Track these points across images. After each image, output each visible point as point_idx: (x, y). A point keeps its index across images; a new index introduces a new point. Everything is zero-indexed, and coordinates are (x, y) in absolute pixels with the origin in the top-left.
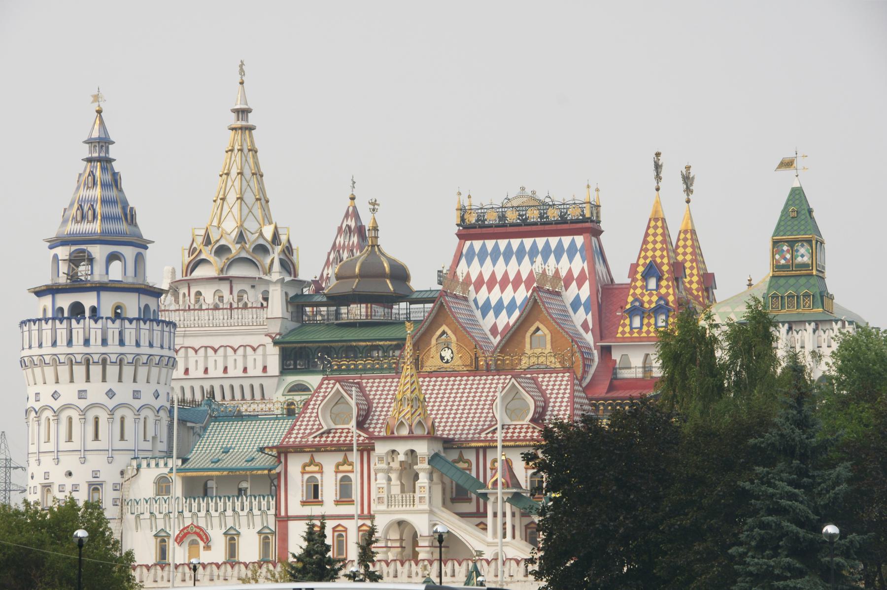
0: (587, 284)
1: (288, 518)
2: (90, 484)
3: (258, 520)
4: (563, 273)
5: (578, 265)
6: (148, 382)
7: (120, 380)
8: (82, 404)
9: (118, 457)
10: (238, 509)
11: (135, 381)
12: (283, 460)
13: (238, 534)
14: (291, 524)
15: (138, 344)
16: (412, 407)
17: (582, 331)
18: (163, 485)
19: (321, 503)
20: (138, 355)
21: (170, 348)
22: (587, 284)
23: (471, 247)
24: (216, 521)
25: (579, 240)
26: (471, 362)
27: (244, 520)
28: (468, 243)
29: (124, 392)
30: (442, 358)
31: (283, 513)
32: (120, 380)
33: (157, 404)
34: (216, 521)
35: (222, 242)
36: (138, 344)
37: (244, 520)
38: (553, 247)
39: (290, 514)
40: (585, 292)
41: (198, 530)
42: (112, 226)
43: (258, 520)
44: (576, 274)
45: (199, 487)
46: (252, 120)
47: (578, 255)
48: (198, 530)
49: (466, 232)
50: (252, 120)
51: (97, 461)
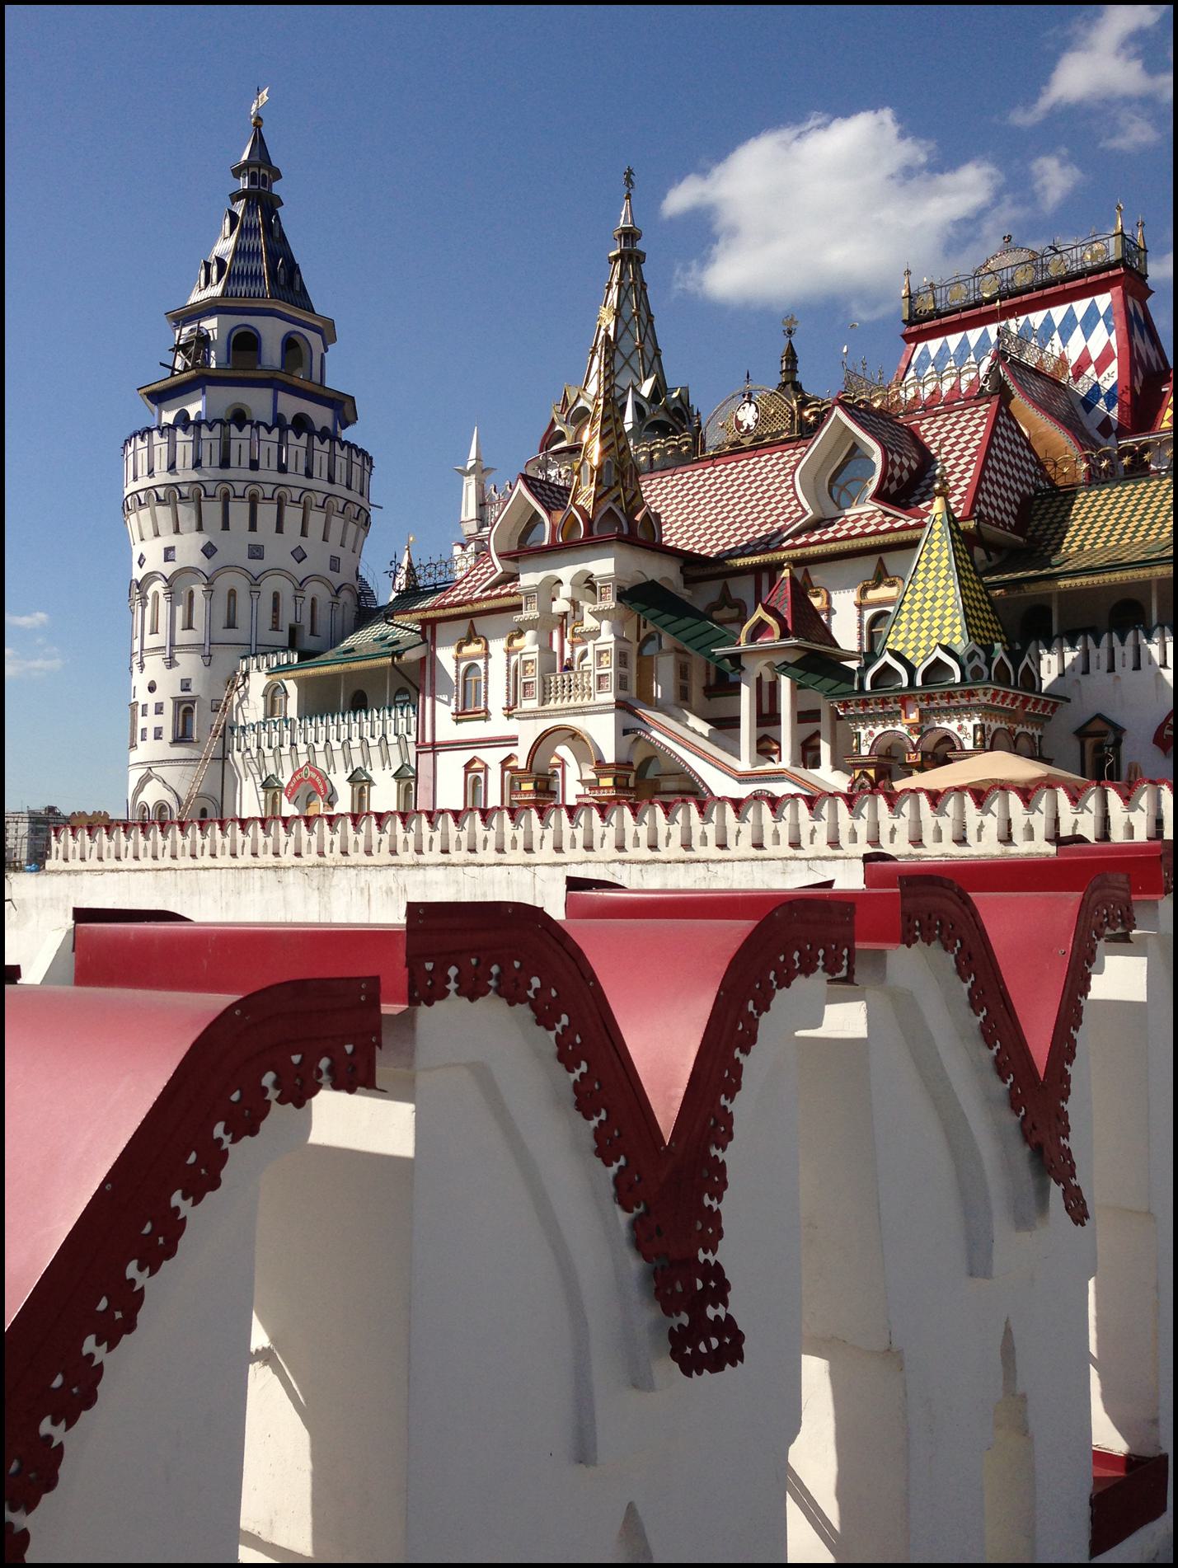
0: (1114, 366)
1: (435, 748)
2: (178, 702)
3: (394, 753)
4: (1073, 356)
5: (1101, 339)
6: (279, 530)
7: (226, 526)
8: (168, 569)
9: (220, 654)
10: (367, 735)
11: (253, 527)
12: (428, 637)
13: (370, 782)
14: (443, 757)
15: (254, 465)
16: (598, 484)
17: (1097, 436)
18: (273, 695)
19: (486, 716)
20: (254, 482)
21: (349, 487)
22: (1114, 366)
23: (926, 352)
24: (339, 757)
25: (1103, 301)
26: (792, 424)
27: (375, 754)
28: (921, 346)
29: (235, 545)
30: (739, 424)
31: (428, 740)
32: (226, 526)
33: (301, 570)
34: (339, 757)
35: (581, 403)
36: (254, 465)
37: (375, 754)
38: (1057, 322)
39: (438, 739)
40: (1109, 378)
41: (314, 775)
42: (243, 288)
43: (394, 753)
44: (1095, 355)
45: (323, 701)
46: (640, 245)
47: (1101, 324)
48: (314, 775)
49: (914, 329)
50: (640, 245)
51: (188, 664)
